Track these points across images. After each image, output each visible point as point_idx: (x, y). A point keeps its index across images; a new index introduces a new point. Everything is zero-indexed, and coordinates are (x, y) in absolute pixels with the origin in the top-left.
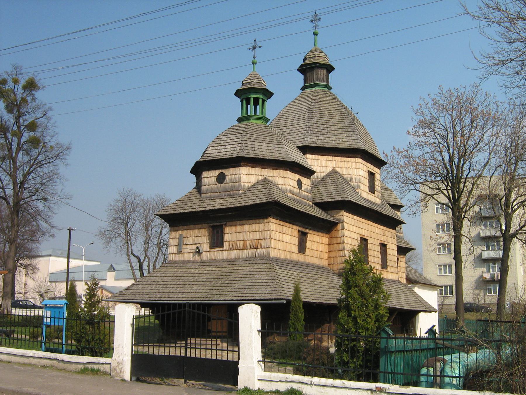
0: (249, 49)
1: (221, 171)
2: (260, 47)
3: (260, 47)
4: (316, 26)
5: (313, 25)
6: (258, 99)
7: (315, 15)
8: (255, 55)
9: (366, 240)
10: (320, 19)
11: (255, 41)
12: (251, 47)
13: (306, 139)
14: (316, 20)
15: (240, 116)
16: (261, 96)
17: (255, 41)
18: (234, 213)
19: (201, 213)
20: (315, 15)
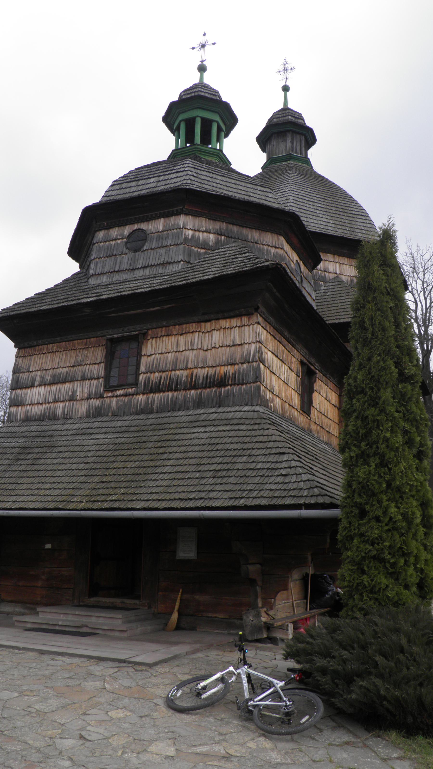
0: (193, 48)
1: (136, 227)
2: (214, 44)
3: (214, 44)
4: (286, 79)
8: (203, 55)
10: (292, 69)
11: (204, 35)
14: (286, 70)
15: (174, 149)
16: (216, 118)
17: (204, 35)
18: (166, 307)
19: (87, 311)
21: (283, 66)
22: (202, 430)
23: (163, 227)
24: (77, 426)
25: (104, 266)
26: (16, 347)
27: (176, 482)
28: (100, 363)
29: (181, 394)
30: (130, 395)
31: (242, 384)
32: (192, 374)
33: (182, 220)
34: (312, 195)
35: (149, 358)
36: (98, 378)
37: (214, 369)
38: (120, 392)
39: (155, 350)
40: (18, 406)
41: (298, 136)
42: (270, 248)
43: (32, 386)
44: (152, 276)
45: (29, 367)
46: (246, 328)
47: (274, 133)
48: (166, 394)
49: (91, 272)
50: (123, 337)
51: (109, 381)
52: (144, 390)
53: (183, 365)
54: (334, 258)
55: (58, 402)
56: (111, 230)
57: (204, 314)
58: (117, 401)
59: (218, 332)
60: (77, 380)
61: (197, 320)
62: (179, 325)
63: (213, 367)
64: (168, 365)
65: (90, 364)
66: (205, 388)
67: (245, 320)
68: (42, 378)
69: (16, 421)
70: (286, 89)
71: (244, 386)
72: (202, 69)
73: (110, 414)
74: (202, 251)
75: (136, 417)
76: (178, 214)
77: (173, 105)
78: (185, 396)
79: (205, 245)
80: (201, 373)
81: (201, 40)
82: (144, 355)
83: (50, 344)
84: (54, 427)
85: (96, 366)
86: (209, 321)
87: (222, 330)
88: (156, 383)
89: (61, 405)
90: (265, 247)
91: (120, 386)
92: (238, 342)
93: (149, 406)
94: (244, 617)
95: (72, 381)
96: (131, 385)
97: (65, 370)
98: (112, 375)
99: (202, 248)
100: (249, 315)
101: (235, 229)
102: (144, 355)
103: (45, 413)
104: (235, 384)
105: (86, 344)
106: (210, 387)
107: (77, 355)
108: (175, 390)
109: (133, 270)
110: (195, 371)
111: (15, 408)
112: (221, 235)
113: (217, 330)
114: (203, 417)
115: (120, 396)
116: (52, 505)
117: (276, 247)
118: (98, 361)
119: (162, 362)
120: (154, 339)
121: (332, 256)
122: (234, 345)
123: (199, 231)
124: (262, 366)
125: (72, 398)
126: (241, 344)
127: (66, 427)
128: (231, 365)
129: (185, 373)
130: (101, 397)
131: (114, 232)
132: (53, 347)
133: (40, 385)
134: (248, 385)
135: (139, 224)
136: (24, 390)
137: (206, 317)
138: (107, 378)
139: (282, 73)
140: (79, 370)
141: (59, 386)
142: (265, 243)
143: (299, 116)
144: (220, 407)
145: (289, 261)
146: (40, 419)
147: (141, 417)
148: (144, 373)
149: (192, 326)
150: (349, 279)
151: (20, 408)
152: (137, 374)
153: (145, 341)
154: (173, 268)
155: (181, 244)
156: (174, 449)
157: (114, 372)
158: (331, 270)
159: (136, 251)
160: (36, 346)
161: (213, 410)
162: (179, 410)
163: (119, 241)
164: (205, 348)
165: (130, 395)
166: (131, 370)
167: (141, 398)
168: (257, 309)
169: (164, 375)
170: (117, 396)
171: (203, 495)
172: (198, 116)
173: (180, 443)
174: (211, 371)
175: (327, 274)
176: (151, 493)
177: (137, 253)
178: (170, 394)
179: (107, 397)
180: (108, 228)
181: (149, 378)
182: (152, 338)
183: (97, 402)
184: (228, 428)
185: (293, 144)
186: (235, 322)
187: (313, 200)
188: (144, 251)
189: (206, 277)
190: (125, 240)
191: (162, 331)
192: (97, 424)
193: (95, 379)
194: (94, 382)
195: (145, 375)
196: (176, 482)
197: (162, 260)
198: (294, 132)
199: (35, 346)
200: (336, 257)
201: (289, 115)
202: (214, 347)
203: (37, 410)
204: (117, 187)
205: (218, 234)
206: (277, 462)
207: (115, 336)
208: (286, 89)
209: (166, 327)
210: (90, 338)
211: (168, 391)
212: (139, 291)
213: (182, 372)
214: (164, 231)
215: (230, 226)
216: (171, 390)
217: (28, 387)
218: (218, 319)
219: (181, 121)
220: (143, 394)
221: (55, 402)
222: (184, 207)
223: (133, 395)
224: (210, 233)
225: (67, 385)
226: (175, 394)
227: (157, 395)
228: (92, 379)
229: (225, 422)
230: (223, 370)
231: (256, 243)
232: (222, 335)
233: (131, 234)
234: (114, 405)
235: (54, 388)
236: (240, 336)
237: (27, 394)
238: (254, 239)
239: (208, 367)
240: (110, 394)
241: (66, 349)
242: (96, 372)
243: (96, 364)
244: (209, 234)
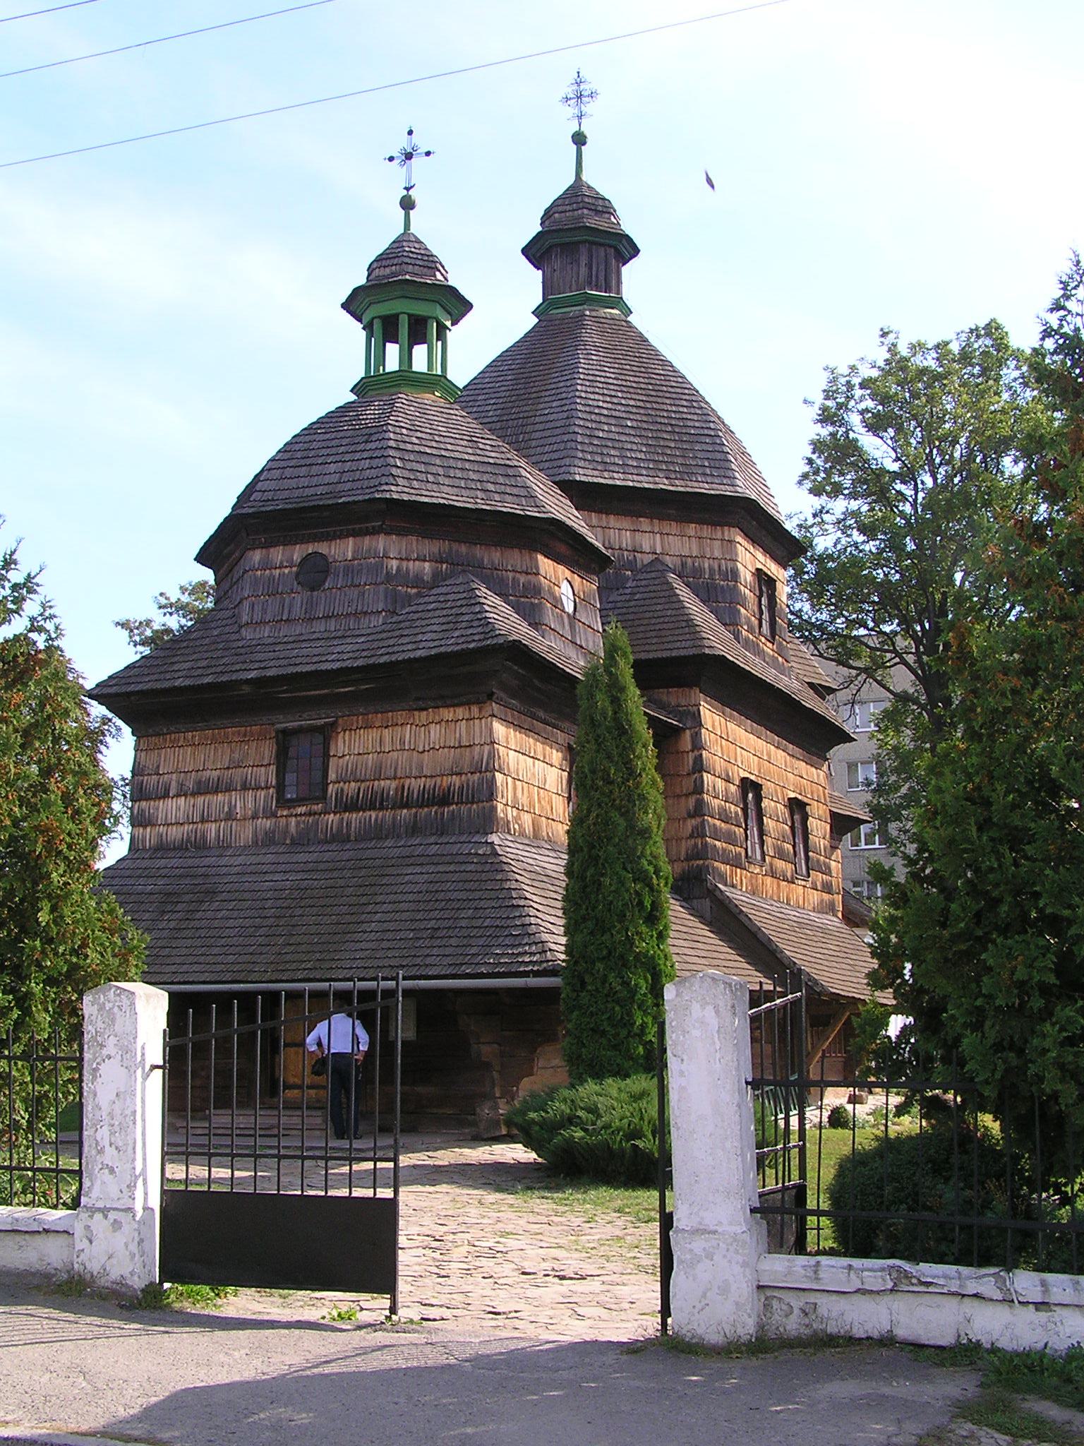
0: (391, 159)
1: (311, 548)
2: (428, 154)
3: (428, 154)
5: (571, 111)
9: (757, 788)
11: (410, 133)
13: (567, 461)
14: (580, 97)
17: (410, 133)
19: (246, 689)
21: (575, 87)
22: (418, 869)
23: (354, 552)
24: (240, 860)
25: (264, 611)
26: (133, 734)
27: (385, 944)
29: (388, 814)
30: (315, 813)
31: (472, 803)
32: (403, 786)
33: (381, 543)
34: (615, 400)
36: (267, 788)
37: (434, 780)
38: (300, 810)
39: (349, 749)
40: (145, 827)
41: (602, 251)
42: (518, 575)
43: (166, 796)
44: (340, 634)
46: (477, 721)
47: (556, 245)
48: (368, 813)
49: (245, 618)
50: (301, 726)
51: (284, 792)
52: (336, 807)
53: (391, 773)
54: (652, 524)
56: (272, 550)
57: (418, 699)
58: (298, 824)
59: (438, 726)
60: (236, 790)
61: (407, 707)
62: (382, 712)
63: (432, 777)
64: (369, 772)
66: (421, 807)
67: (475, 709)
68: (181, 785)
69: (144, 849)
70: (579, 139)
71: (475, 806)
72: (407, 204)
73: (288, 842)
74: (414, 591)
75: (326, 847)
77: (356, 291)
78: (394, 818)
79: (418, 581)
80: (416, 785)
81: (403, 143)
82: (334, 756)
84: (207, 861)
85: (263, 769)
86: (426, 709)
87: (443, 723)
88: (352, 797)
90: (511, 575)
91: (300, 801)
92: (464, 743)
93: (345, 831)
94: (478, 1110)
95: (228, 790)
96: (316, 800)
97: (215, 774)
98: (286, 783)
99: (413, 587)
101: (463, 549)
102: (334, 756)
103: (188, 840)
104: (462, 803)
105: (245, 735)
106: (427, 806)
108: (381, 808)
109: (311, 620)
110: (408, 781)
112: (442, 562)
114: (419, 850)
115: (301, 815)
116: (228, 977)
117: (527, 573)
119: (359, 767)
121: (647, 521)
123: (408, 560)
124: (499, 776)
125: (230, 816)
126: (470, 746)
127: (224, 861)
128: (456, 774)
129: (394, 784)
130: (274, 815)
131: (278, 554)
132: (193, 737)
133: (178, 795)
134: (481, 805)
136: (152, 803)
138: (280, 788)
139: (573, 101)
140: (237, 775)
141: (208, 797)
142: (509, 568)
144: (442, 834)
145: (549, 586)
146: (181, 847)
147: (333, 847)
149: (401, 715)
150: (678, 561)
151: (148, 829)
153: (334, 734)
154: (370, 622)
156: (380, 898)
157: (290, 778)
158: (646, 548)
159: (312, 589)
161: (432, 840)
162: (387, 838)
163: (286, 571)
164: (421, 749)
165: (315, 813)
166: (317, 775)
168: (490, 696)
170: (296, 815)
171: (418, 961)
173: (389, 889)
174: (430, 783)
175: (638, 555)
176: (355, 959)
177: (315, 593)
178: (374, 814)
180: (268, 545)
181: (342, 790)
182: (345, 731)
183: (269, 823)
184: (452, 868)
185: (590, 268)
186: (461, 712)
187: (617, 414)
189: (419, 654)
190: (295, 569)
192: (270, 858)
194: (262, 794)
195: (336, 786)
196: (385, 944)
197: (354, 607)
199: (163, 734)
200: (656, 521)
201: (583, 208)
203: (175, 833)
204: (277, 473)
205: (436, 562)
206: (508, 918)
208: (579, 139)
210: (251, 726)
211: (370, 810)
212: (324, 667)
213: (388, 782)
214: (354, 559)
215: (455, 546)
216: (374, 809)
220: (335, 813)
221: (202, 821)
222: (384, 523)
224: (425, 561)
227: (354, 815)
229: (448, 859)
230: (446, 781)
231: (496, 569)
232: (443, 731)
233: (305, 560)
234: (293, 829)
235: (200, 800)
236: (468, 733)
237: (158, 809)
238: (493, 563)
241: (214, 740)
242: (263, 779)
243: (262, 766)
244: (421, 563)
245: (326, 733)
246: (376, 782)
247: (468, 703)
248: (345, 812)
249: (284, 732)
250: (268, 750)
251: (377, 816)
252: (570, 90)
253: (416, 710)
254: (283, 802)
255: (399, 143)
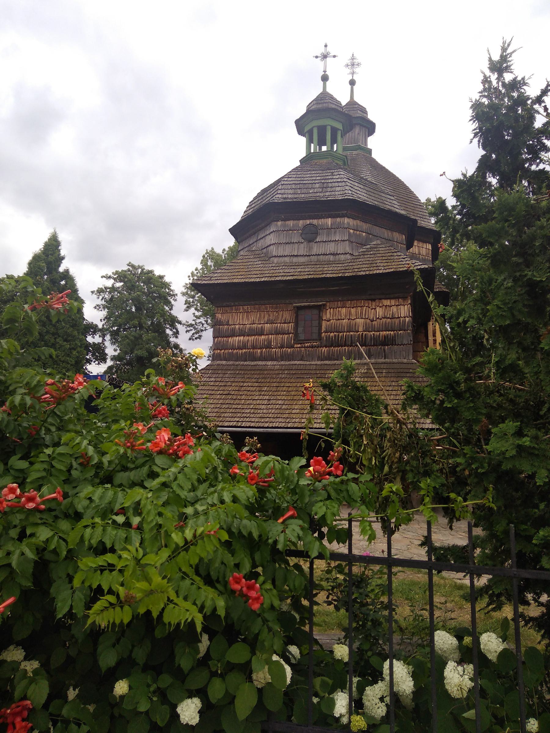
1: (308, 222)
2: (334, 56)
3: (334, 56)
4: (353, 73)
5: (348, 71)
6: (339, 129)
7: (353, 58)
8: (325, 66)
10: (358, 65)
11: (326, 46)
12: (319, 55)
14: (353, 65)
17: (326, 46)
20: (353, 58)
23: (331, 224)
28: (290, 323)
35: (328, 323)
40: (221, 350)
41: (364, 128)
45: (228, 321)
46: (402, 307)
48: (344, 348)
55: (256, 348)
57: (370, 295)
62: (351, 301)
65: (280, 323)
70: (352, 83)
72: (325, 78)
76: (343, 216)
81: (322, 50)
83: (245, 305)
86: (374, 300)
89: (259, 351)
91: (307, 340)
97: (260, 326)
100: (404, 298)
106: (377, 345)
107: (269, 316)
110: (364, 333)
111: (219, 351)
112: (370, 234)
113: (380, 307)
115: (307, 347)
118: (289, 321)
120: (332, 309)
122: (393, 318)
131: (291, 223)
135: (311, 220)
136: (225, 339)
137: (373, 297)
138: (296, 334)
143: (364, 110)
144: (385, 359)
148: (326, 333)
151: (223, 351)
152: (320, 333)
155: (346, 240)
157: (300, 330)
160: (233, 306)
165: (315, 347)
166: (315, 330)
167: (324, 349)
169: (340, 334)
170: (305, 347)
172: (329, 125)
178: (347, 348)
179: (297, 347)
181: (329, 335)
182: (330, 308)
186: (393, 302)
188: (316, 242)
191: (338, 304)
193: (286, 334)
198: (361, 125)
202: (378, 318)
207: (303, 304)
208: (352, 83)
209: (341, 301)
216: (348, 346)
217: (229, 337)
218: (380, 299)
219: (314, 127)
221: (254, 347)
223: (318, 347)
225: (263, 337)
226: (350, 348)
227: (336, 348)
228: (283, 334)
233: (305, 227)
239: (374, 331)
240: (299, 346)
241: (259, 310)
243: (285, 323)
245: (320, 308)
246: (348, 333)
247: (398, 298)
248: (331, 346)
249: (299, 308)
250: (287, 315)
251: (348, 349)
252: (349, 61)
253: (369, 300)
254: (297, 340)
255: (321, 50)
